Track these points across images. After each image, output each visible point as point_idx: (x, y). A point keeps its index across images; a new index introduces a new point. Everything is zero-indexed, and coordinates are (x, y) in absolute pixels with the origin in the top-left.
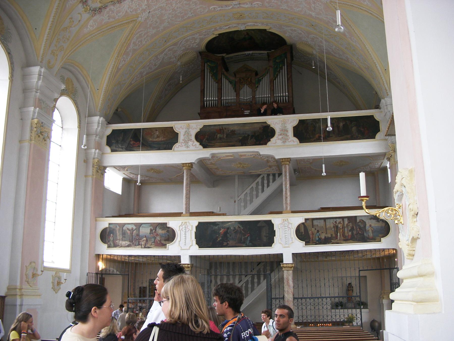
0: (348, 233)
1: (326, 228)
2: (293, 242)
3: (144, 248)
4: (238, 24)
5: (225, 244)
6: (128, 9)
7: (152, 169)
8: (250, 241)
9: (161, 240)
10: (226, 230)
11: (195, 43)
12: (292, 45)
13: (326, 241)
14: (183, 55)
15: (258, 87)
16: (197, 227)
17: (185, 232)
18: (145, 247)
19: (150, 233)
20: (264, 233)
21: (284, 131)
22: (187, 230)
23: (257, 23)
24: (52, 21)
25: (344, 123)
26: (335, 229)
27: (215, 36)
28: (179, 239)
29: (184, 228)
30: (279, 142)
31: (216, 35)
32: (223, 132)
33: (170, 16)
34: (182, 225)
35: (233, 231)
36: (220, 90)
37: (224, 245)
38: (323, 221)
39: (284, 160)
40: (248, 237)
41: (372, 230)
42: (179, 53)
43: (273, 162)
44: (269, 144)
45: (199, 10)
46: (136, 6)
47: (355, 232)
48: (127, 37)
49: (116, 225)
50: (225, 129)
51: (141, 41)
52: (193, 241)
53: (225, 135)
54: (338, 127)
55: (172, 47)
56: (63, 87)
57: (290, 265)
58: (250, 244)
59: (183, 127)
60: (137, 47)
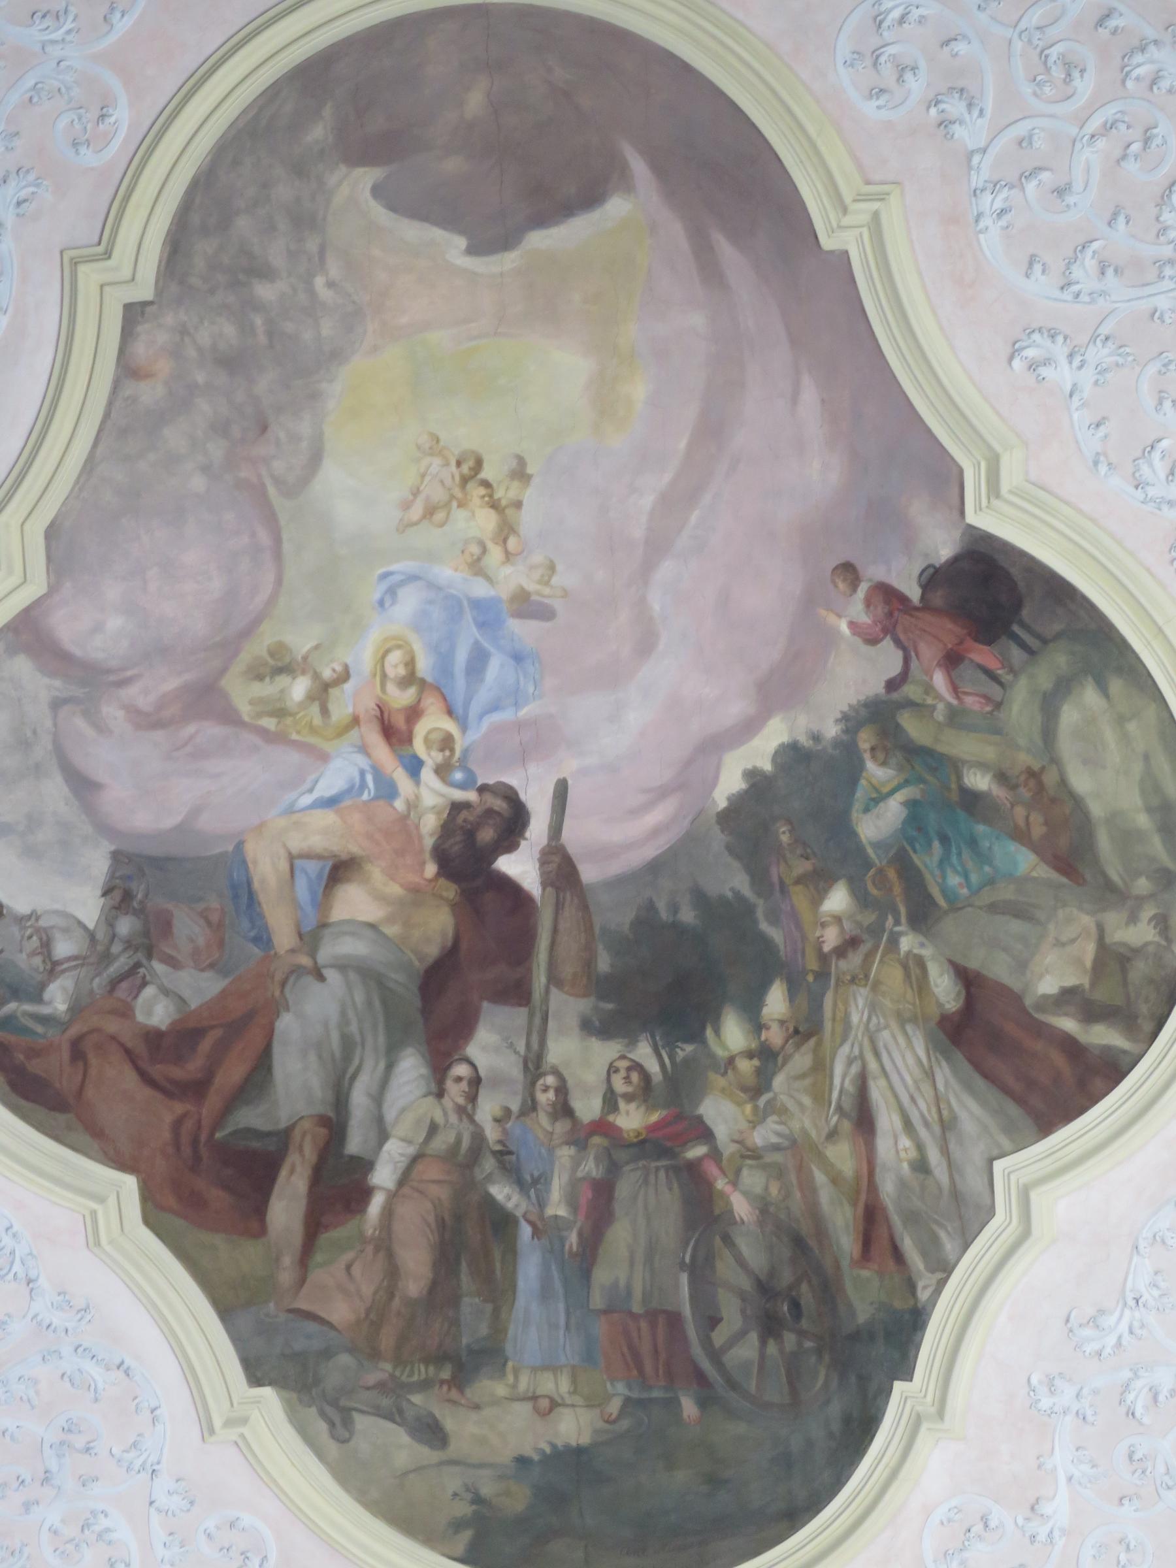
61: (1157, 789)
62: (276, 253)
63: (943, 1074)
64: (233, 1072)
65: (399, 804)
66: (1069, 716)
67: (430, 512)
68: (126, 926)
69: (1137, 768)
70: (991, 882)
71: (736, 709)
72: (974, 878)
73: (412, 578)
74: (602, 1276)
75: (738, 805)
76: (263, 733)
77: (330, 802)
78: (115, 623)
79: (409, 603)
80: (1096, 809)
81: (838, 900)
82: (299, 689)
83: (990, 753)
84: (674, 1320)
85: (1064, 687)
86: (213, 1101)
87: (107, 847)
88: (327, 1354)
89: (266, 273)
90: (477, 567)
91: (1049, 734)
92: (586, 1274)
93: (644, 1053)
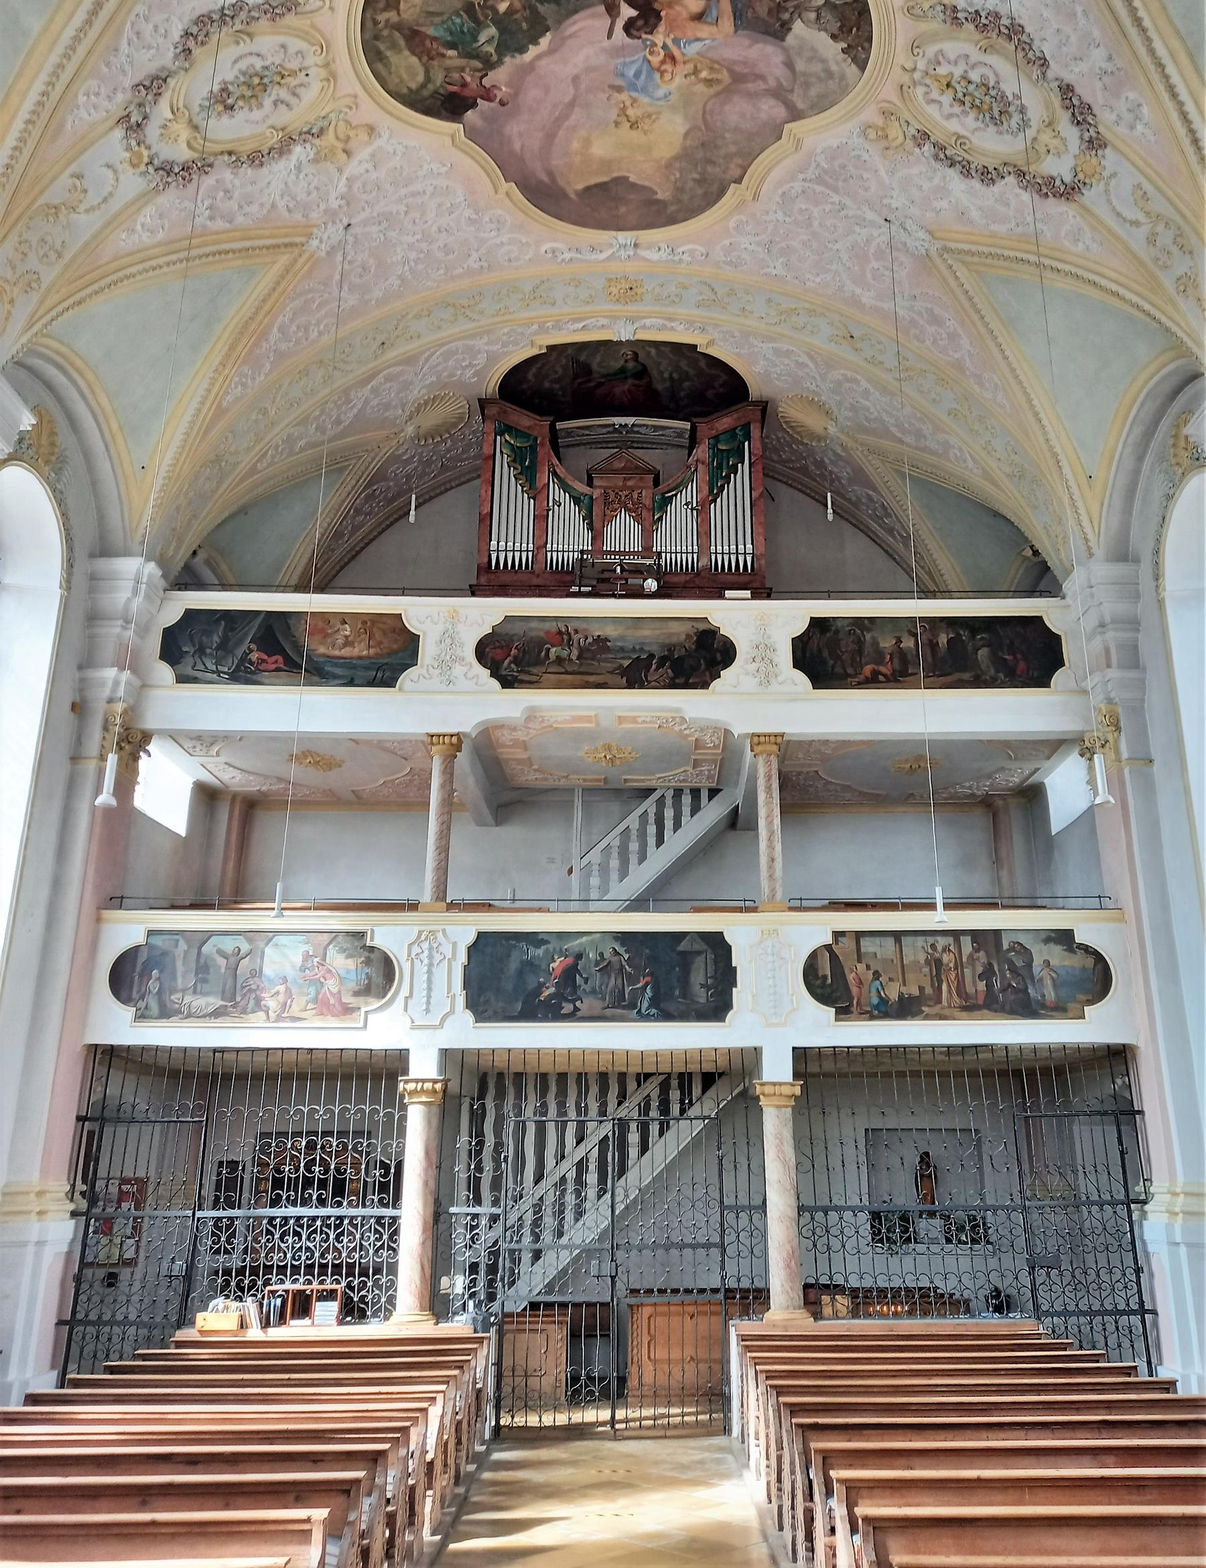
0: (975, 984)
1: (903, 966)
3: (276, 1021)
5: (567, 1008)
6: (282, 196)
7: (309, 752)
8: (654, 1002)
9: (339, 992)
10: (570, 960)
11: (470, 365)
12: (767, 402)
13: (905, 1009)
14: (426, 403)
15: (660, 519)
16: (472, 950)
17: (430, 965)
20: (699, 976)
21: (764, 650)
22: (438, 957)
23: (671, 320)
25: (951, 635)
26: (931, 970)
27: (535, 352)
29: (426, 953)
30: (750, 683)
31: (541, 348)
32: (570, 639)
33: (413, 255)
34: (418, 941)
35: (596, 966)
38: (890, 942)
39: (762, 739)
40: (644, 988)
41: (1052, 978)
42: (416, 392)
44: (716, 684)
45: (504, 249)
46: (309, 194)
48: (264, 301)
49: (176, 937)
50: (576, 632)
51: (306, 330)
52: (457, 997)
53: (575, 653)
55: (400, 368)
58: (654, 1011)
60: (291, 344)
61: (385, 65)
62: (690, 184)
65: (672, 36)
66: (421, 78)
67: (649, 116)
68: (786, 16)
69: (393, 69)
70: (443, 22)
71: (543, 63)
72: (450, 23)
73: (658, 99)
75: (543, 34)
76: (718, 63)
77: (698, 39)
78: (765, 107)
79: (660, 93)
80: (407, 53)
82: (704, 74)
83: (448, 63)
85: (423, 86)
87: (785, 44)
89: (695, 180)
90: (634, 101)
91: (427, 72)
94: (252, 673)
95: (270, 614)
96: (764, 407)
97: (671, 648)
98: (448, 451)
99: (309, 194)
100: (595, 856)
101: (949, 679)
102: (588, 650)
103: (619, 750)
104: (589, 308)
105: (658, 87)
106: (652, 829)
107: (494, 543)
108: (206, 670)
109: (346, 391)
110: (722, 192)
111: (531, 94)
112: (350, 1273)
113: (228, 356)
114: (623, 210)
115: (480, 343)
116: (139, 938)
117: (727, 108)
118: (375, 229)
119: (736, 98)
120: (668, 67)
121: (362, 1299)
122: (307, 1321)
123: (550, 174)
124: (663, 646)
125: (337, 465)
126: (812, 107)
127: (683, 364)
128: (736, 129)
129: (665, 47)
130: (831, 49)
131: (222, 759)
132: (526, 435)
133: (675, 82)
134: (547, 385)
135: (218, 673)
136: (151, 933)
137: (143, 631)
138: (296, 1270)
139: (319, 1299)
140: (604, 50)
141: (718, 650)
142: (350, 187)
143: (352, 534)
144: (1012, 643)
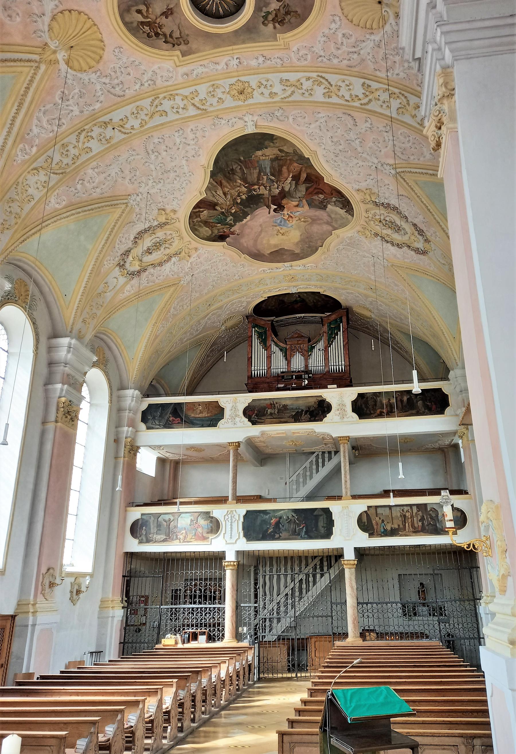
2: (354, 534)
4: (290, 287)
14: (227, 319)
18: (184, 542)
19: (190, 525)
24: (85, 287)
28: (223, 532)
30: (337, 418)
33: (216, 279)
36: (269, 357)
37: (276, 537)
43: (330, 439)
46: (178, 269)
47: (426, 523)
48: (167, 302)
53: (276, 411)
54: (402, 401)
56: (95, 359)
57: (352, 562)
59: (229, 401)
63: (216, 201)
64: (311, 190)
66: (210, 233)
68: (325, 204)
71: (249, 223)
74: (258, 171)
79: (289, 226)
81: (233, 211)
82: (302, 220)
84: (246, 168)
85: (212, 234)
86: (315, 186)
88: (297, 160)
91: (212, 231)
92: (260, 171)
93: (255, 193)
94: (171, 424)
95: (176, 404)
96: (348, 310)
97: (309, 408)
98: (238, 332)
99: (178, 269)
100: (294, 478)
101: (407, 413)
102: (281, 410)
103: (297, 442)
104: (279, 285)
105: (288, 224)
106: (314, 467)
107: (253, 367)
108: (156, 425)
109: (199, 321)
110: (317, 250)
111: (247, 231)
112: (210, 626)
113: (157, 320)
114: (285, 257)
115: (243, 299)
116: (139, 516)
117: (312, 228)
118: (202, 274)
119: (314, 225)
120: (290, 219)
121: (214, 635)
122: (197, 642)
123: (258, 251)
124: (306, 407)
125: (197, 344)
126: (340, 226)
127: (317, 297)
128: (317, 233)
129: (288, 214)
130: (342, 212)
131: (165, 450)
132: (263, 328)
133: (294, 222)
134: (269, 308)
135: (159, 425)
136: (142, 515)
137: (135, 413)
138: (192, 626)
139: (200, 635)
140: (268, 217)
141: (325, 407)
142: (192, 265)
143: (207, 364)
144: (430, 399)
